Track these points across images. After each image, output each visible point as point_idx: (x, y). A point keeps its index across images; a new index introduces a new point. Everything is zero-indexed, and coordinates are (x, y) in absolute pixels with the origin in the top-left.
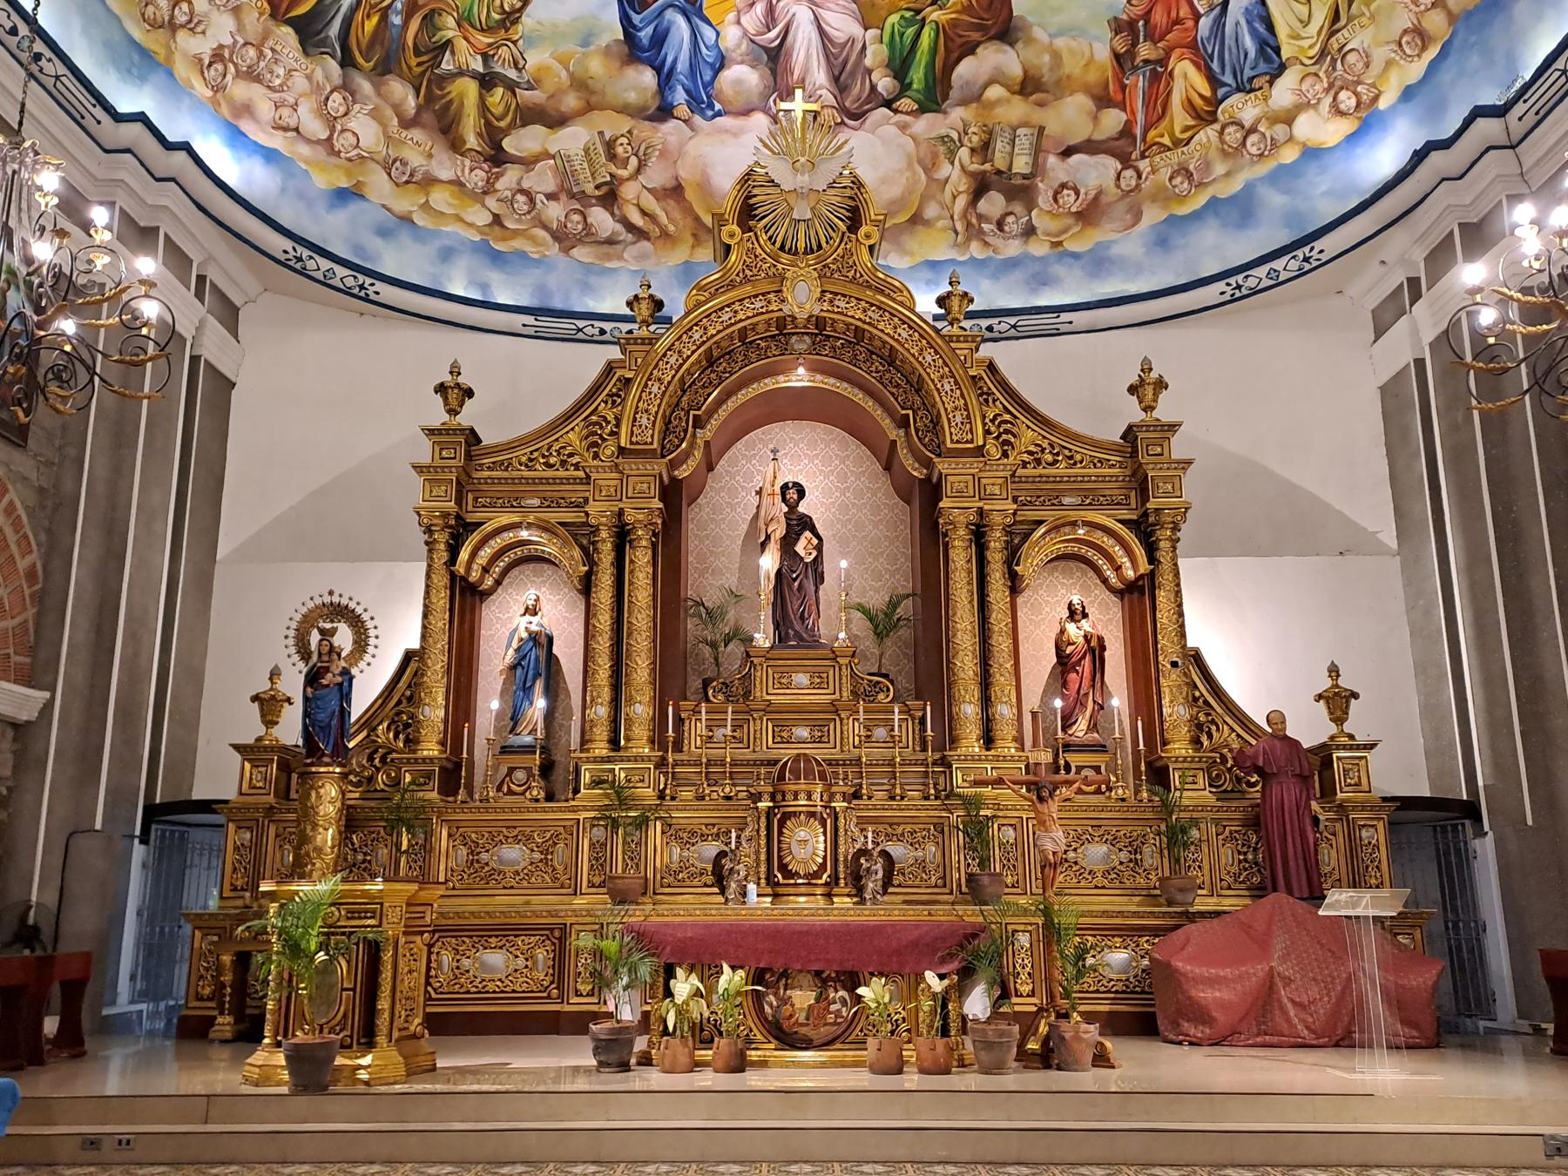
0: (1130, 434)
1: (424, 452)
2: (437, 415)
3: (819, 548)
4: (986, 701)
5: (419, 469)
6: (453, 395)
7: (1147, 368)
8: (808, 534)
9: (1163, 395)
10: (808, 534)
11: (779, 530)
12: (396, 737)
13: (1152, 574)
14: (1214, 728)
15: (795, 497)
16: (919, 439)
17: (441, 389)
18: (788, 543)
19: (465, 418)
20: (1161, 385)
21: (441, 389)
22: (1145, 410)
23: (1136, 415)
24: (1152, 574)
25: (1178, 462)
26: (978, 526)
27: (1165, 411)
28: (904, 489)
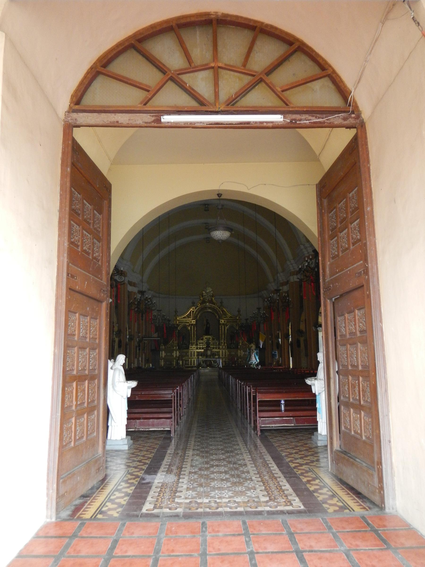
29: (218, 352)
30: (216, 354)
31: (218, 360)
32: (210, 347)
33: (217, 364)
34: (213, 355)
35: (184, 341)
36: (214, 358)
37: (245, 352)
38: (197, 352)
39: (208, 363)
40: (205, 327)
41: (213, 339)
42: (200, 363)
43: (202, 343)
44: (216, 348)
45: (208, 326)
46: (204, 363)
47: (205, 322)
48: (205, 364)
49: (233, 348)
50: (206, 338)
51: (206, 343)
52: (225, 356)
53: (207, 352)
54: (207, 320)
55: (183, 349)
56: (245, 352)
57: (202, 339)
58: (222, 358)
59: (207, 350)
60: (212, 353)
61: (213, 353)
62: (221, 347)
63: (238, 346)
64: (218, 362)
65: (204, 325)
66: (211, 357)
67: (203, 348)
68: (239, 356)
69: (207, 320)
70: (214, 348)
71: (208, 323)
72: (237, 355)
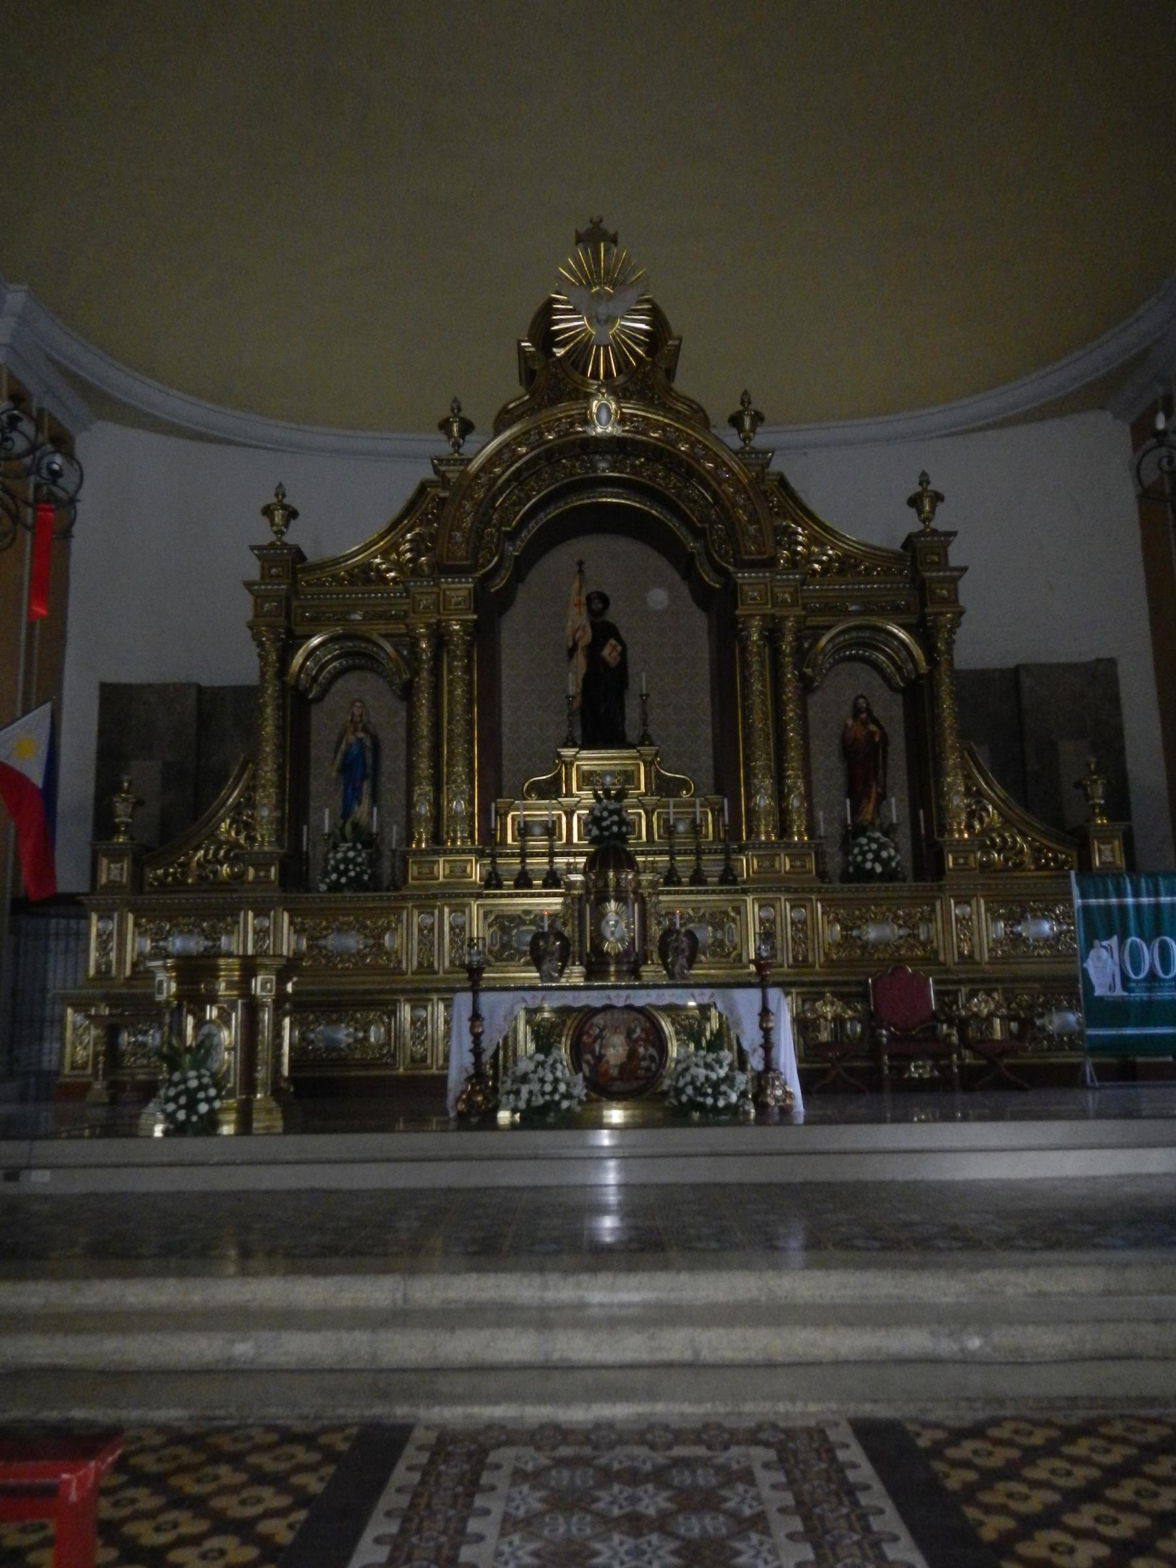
0: (909, 543)
1: (253, 570)
2: (265, 535)
3: (623, 654)
4: (780, 795)
5: (248, 585)
6: (278, 516)
7: (924, 480)
8: (612, 642)
9: (940, 507)
10: (612, 642)
11: (587, 637)
12: (238, 833)
13: (930, 676)
14: (984, 814)
15: (600, 606)
16: (717, 552)
17: (267, 511)
18: (593, 651)
19: (291, 538)
20: (938, 498)
21: (267, 511)
22: (924, 521)
23: (915, 525)
24: (930, 676)
25: (955, 569)
26: (772, 631)
27: (941, 522)
28: (703, 597)
29: (718, 920)
30: (706, 935)
31: (747, 1001)
32: (626, 861)
33: (742, 1061)
34: (663, 956)
35: (361, 811)
36: (676, 980)
37: (1013, 919)
38: (504, 923)
39: (615, 1051)
40: (580, 661)
41: (664, 788)
42: (509, 1043)
43: (551, 830)
44: (698, 878)
45: (609, 653)
46: (563, 1052)
47: (577, 621)
48: (577, 1066)
49: (890, 875)
50: (587, 779)
51: (595, 820)
52: (801, 963)
53: (599, 916)
54: (597, 604)
55: (335, 887)
56: (1013, 919)
57: (550, 790)
58: (785, 986)
59: (602, 898)
60: (656, 931)
61: (668, 933)
62: (747, 864)
63: (940, 859)
64: (751, 1037)
65: (572, 652)
66: (649, 971)
67: (552, 879)
68: (948, 957)
69: (597, 604)
70: (671, 878)
71: (604, 631)
72: (932, 959)
